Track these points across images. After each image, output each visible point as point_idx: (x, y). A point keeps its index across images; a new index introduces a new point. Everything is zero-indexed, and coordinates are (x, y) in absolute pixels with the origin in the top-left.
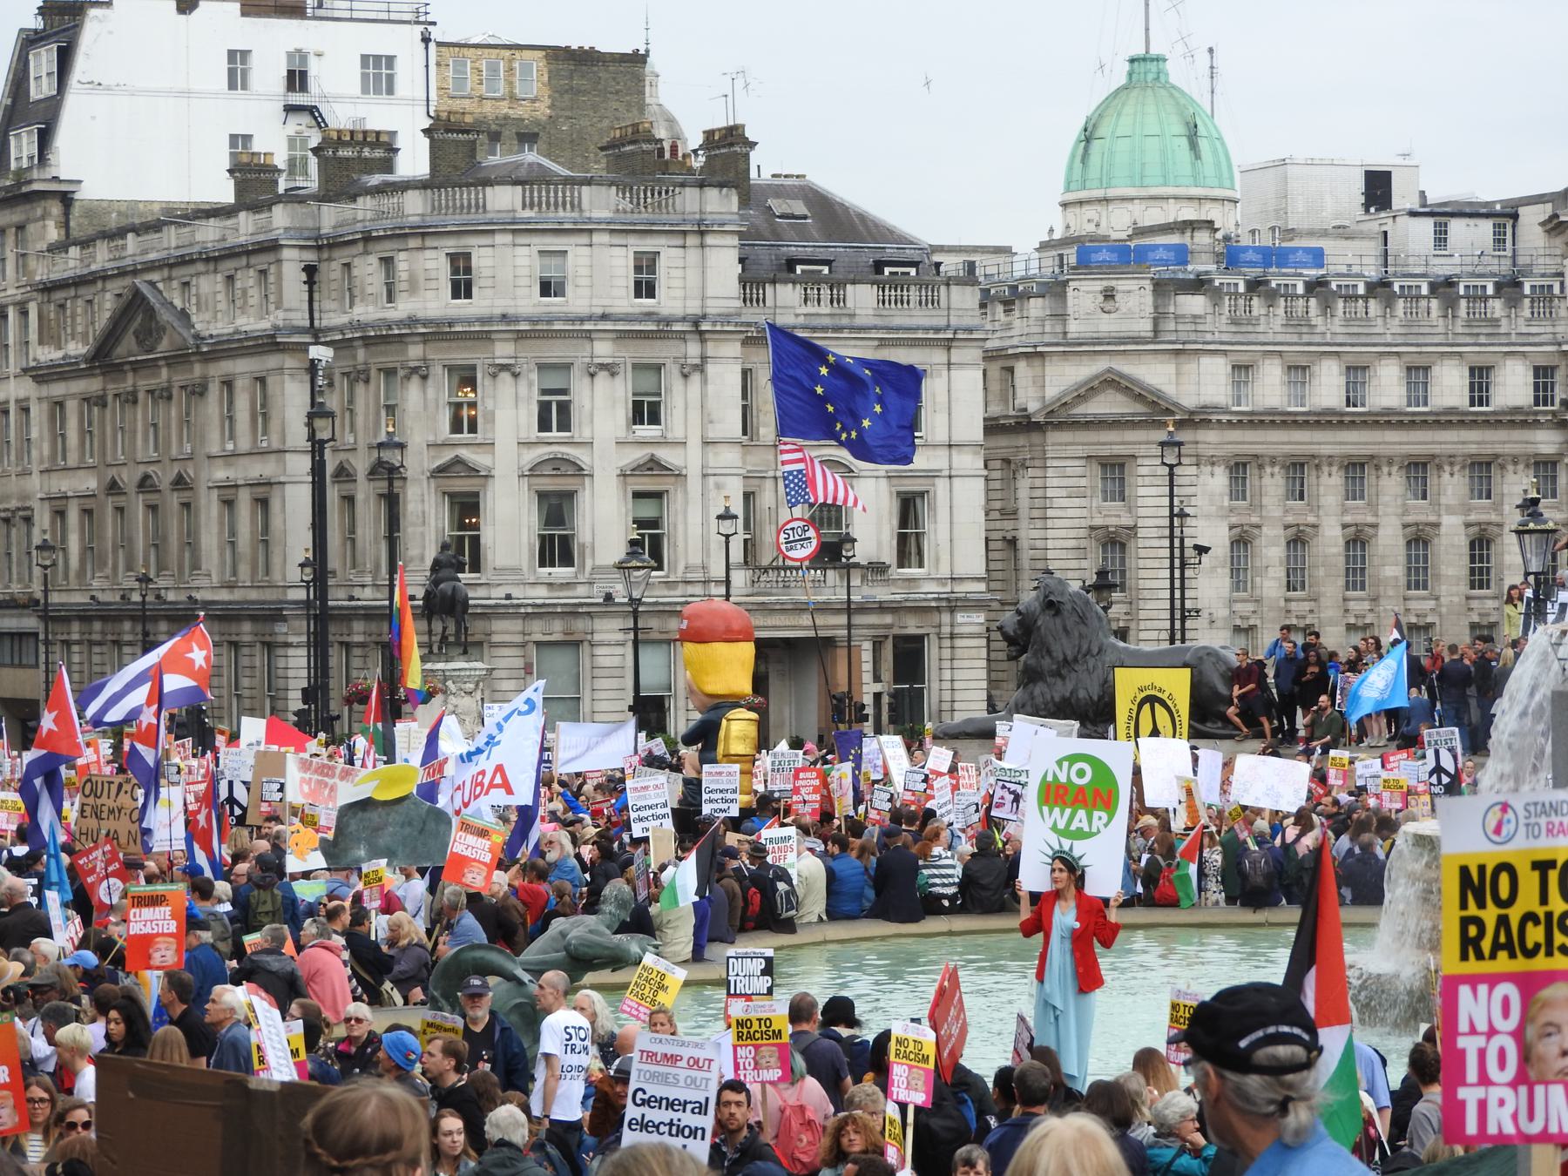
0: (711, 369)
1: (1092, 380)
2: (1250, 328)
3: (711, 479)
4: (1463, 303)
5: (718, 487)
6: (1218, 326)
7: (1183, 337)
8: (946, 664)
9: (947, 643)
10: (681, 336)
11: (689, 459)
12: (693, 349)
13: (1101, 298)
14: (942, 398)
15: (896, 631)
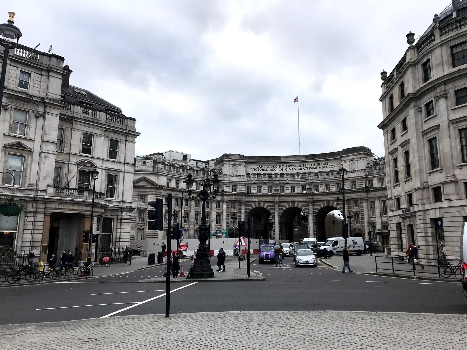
0: (47, 116)
1: (140, 178)
2: (170, 172)
3: (43, 154)
4: (206, 172)
5: (46, 157)
6: (165, 171)
7: (159, 172)
8: (119, 227)
9: (119, 221)
10: (37, 103)
11: (36, 147)
12: (41, 109)
13: (143, 163)
14: (123, 150)
15: (104, 216)
